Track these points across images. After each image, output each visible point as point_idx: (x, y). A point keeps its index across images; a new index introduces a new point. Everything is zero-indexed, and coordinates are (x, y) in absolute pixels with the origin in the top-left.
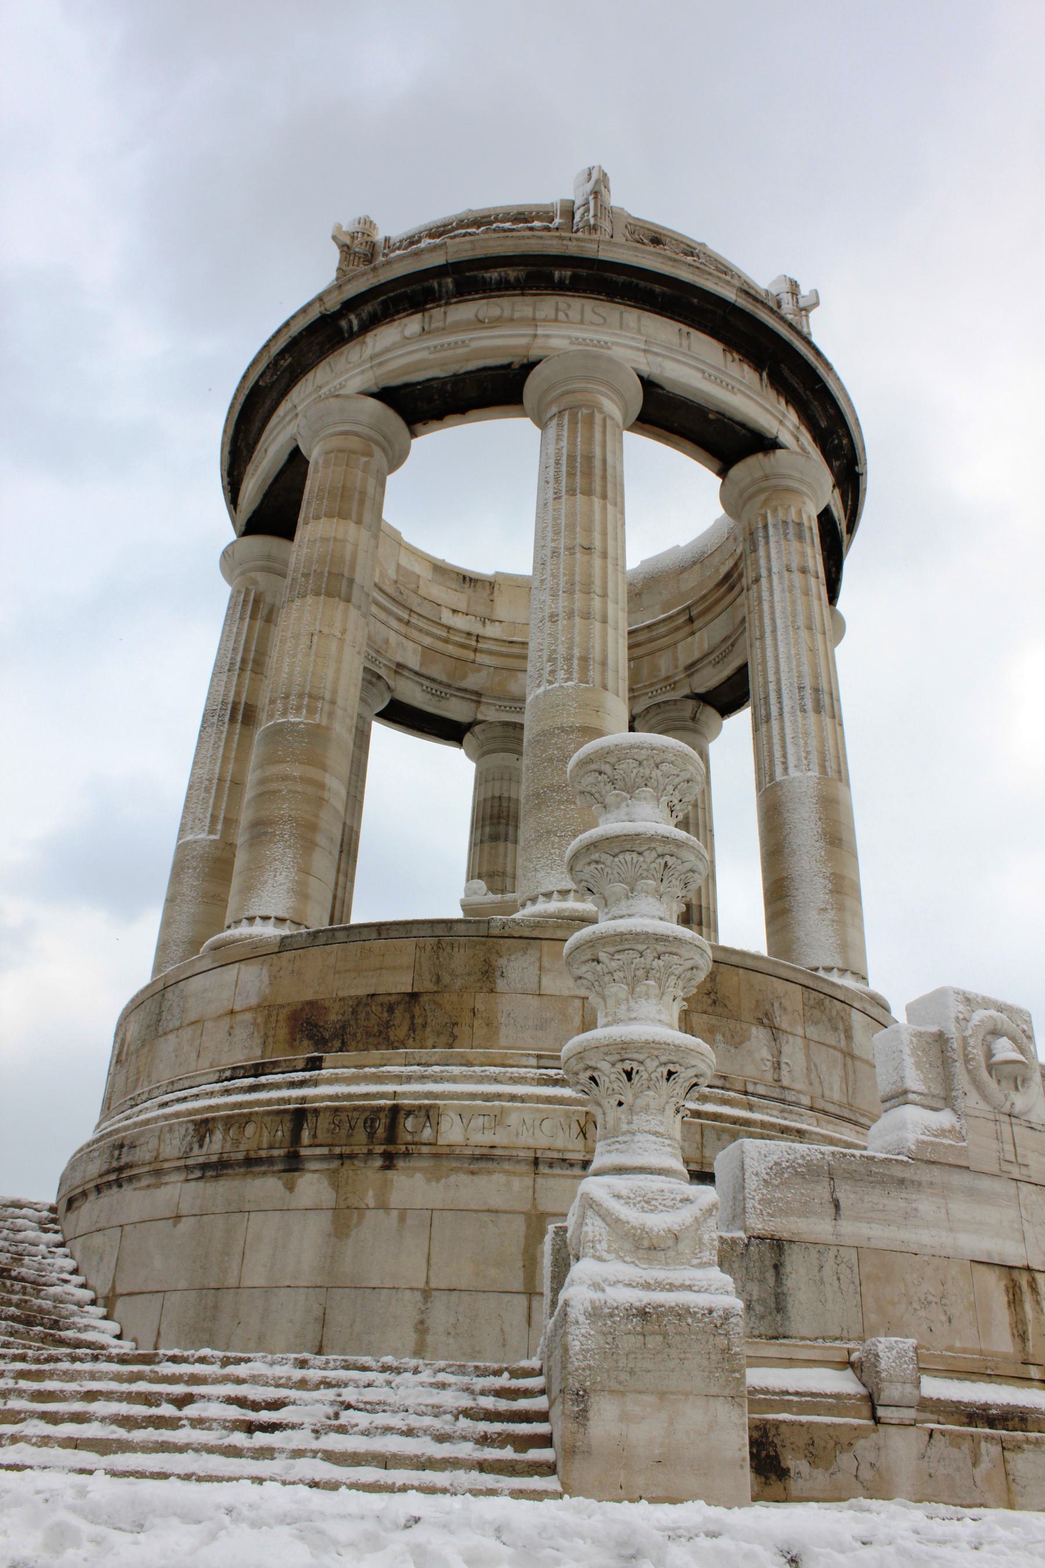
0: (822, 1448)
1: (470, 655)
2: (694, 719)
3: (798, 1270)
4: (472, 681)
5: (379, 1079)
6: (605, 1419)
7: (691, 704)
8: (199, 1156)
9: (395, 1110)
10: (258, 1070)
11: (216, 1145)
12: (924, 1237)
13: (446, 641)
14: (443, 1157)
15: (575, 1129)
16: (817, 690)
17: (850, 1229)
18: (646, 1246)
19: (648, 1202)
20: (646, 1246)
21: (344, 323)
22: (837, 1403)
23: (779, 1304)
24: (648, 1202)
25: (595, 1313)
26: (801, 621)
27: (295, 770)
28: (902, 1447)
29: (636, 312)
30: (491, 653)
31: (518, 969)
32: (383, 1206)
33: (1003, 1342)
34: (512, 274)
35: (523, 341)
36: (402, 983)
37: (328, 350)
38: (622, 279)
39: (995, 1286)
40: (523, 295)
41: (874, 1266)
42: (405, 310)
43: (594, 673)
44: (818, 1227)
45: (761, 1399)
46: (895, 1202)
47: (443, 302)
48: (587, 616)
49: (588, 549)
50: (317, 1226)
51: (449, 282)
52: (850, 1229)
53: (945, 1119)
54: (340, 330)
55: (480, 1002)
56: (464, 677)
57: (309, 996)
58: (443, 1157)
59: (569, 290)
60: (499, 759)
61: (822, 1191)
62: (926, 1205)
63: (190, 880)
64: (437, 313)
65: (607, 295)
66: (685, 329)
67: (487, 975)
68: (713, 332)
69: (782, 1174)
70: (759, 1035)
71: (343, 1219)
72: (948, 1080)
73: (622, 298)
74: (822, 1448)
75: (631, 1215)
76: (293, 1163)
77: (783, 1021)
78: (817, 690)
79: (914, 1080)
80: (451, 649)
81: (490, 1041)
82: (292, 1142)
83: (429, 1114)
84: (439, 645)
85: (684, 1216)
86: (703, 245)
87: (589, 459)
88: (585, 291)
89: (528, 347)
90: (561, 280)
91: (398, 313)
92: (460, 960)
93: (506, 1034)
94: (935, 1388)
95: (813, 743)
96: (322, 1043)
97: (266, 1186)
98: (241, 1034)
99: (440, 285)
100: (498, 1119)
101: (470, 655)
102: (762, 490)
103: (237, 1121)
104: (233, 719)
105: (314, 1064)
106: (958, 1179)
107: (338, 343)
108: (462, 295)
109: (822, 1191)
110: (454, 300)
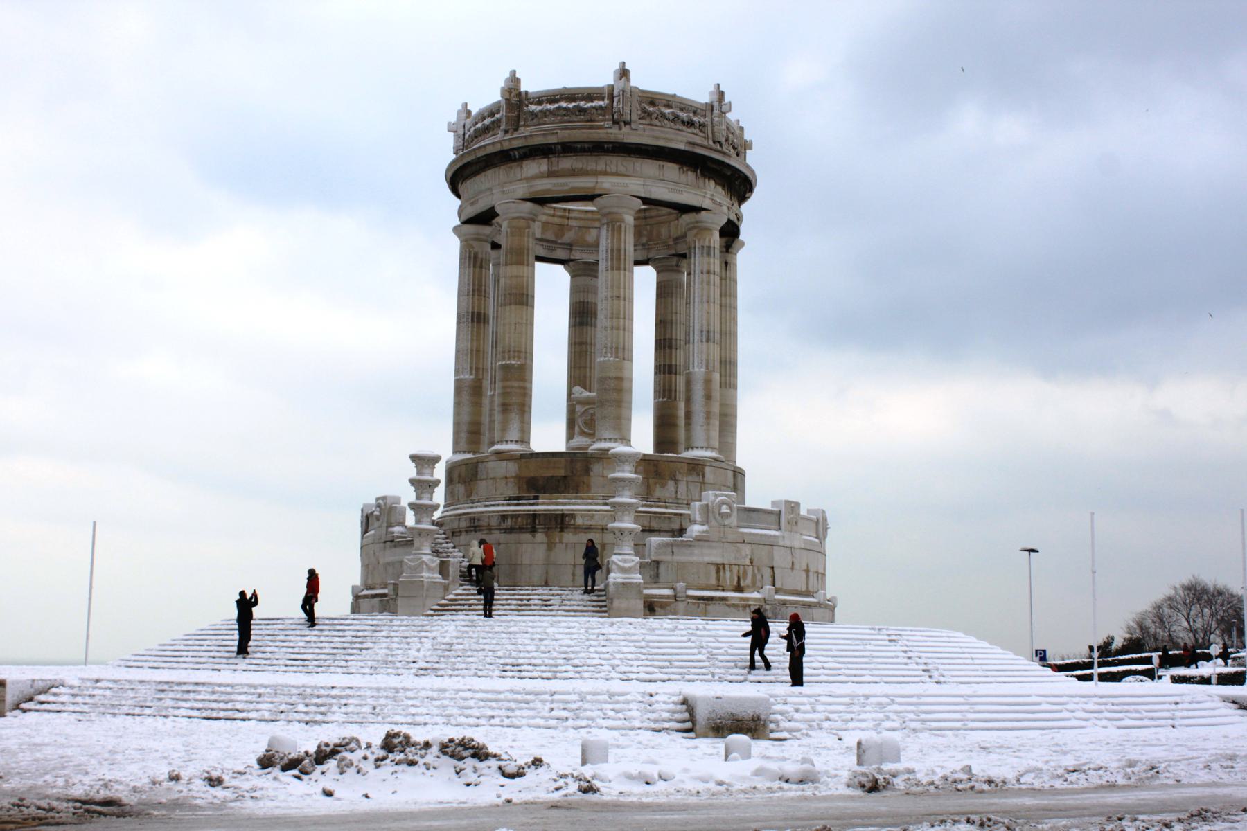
0: (663, 606)
1: (566, 222)
2: (677, 265)
3: (662, 568)
4: (568, 237)
5: (557, 504)
6: (616, 603)
7: (675, 259)
8: (503, 526)
9: (563, 515)
10: (518, 498)
11: (509, 523)
12: (695, 559)
13: (553, 216)
14: (577, 529)
16: (708, 332)
17: (676, 558)
18: (624, 570)
19: (625, 561)
20: (624, 570)
22: (668, 597)
23: (657, 575)
24: (625, 561)
25: (615, 584)
26: (705, 298)
27: (516, 384)
28: (681, 606)
29: (640, 160)
30: (576, 219)
31: (596, 468)
32: (561, 542)
33: (713, 581)
35: (591, 185)
36: (562, 473)
39: (713, 569)
41: (682, 566)
43: (621, 355)
44: (668, 558)
45: (648, 596)
46: (688, 551)
48: (618, 329)
49: (618, 297)
50: (544, 547)
52: (676, 558)
53: (705, 528)
55: (585, 479)
56: (563, 235)
57: (532, 475)
58: (577, 529)
60: (582, 280)
61: (670, 550)
62: (696, 551)
63: (466, 397)
64: (554, 160)
66: (661, 163)
67: (587, 471)
69: (660, 546)
70: (671, 483)
71: (550, 546)
72: (708, 517)
74: (663, 606)
75: (621, 564)
76: (533, 530)
77: (679, 477)
78: (708, 332)
79: (698, 518)
80: (556, 220)
81: (589, 491)
82: (533, 523)
83: (572, 516)
84: (551, 219)
85: (632, 564)
86: (674, 96)
87: (619, 250)
89: (594, 188)
92: (579, 466)
93: (594, 489)
94: (691, 593)
95: (704, 356)
96: (538, 491)
97: (527, 536)
98: (510, 485)
100: (592, 517)
101: (566, 222)
102: (694, 228)
103: (515, 516)
104: (473, 321)
105: (536, 498)
106: (706, 544)
109: (670, 550)
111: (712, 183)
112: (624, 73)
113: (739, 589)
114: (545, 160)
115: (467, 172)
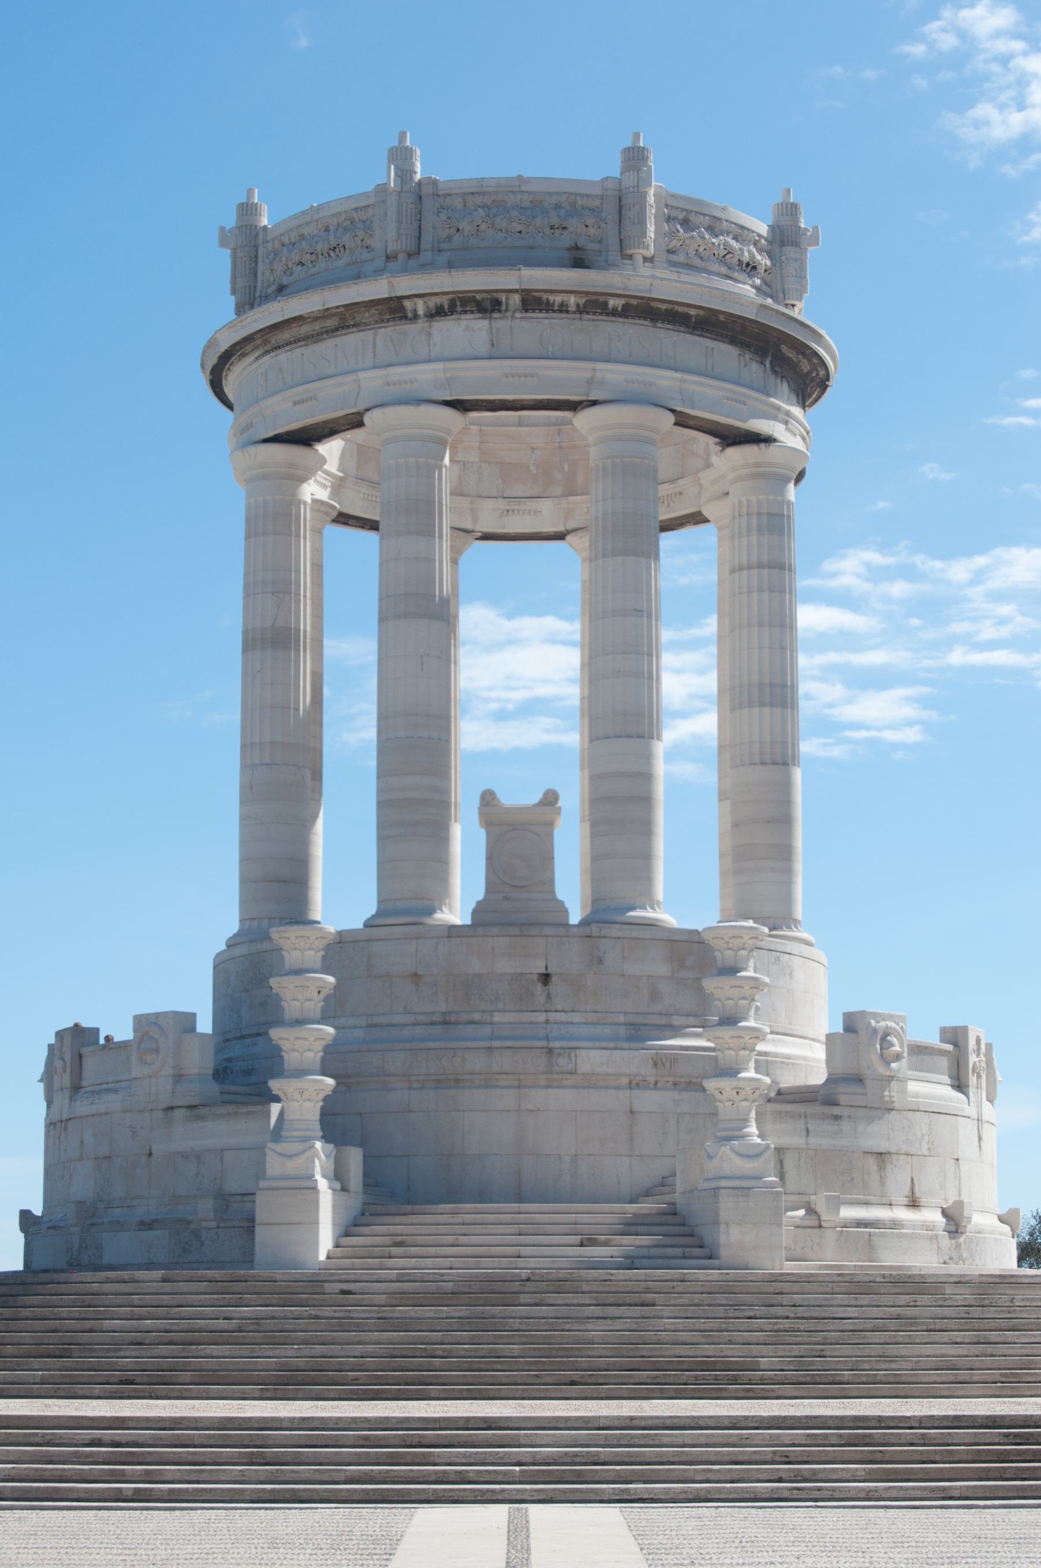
15: (651, 1063)
17: (813, 1141)
21: (408, 304)
34: (572, 300)
37: (388, 320)
38: (664, 307)
40: (581, 319)
42: (472, 312)
44: (799, 1141)
47: (509, 314)
51: (516, 299)
54: (402, 309)
59: (620, 316)
61: (801, 1124)
62: (845, 1126)
65: (652, 320)
68: (733, 341)
73: (663, 323)
88: (633, 317)
90: (615, 309)
91: (465, 312)
99: (507, 299)
107: (401, 318)
108: (527, 311)
110: (518, 315)
111: (785, 385)
112: (635, 158)
113: (914, 1204)
114: (484, 323)
115: (286, 335)
